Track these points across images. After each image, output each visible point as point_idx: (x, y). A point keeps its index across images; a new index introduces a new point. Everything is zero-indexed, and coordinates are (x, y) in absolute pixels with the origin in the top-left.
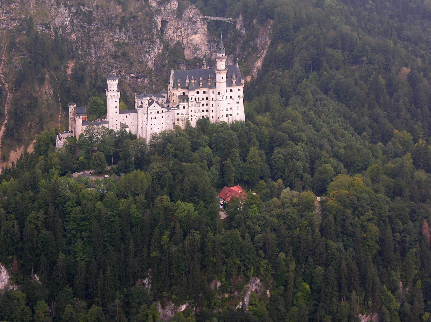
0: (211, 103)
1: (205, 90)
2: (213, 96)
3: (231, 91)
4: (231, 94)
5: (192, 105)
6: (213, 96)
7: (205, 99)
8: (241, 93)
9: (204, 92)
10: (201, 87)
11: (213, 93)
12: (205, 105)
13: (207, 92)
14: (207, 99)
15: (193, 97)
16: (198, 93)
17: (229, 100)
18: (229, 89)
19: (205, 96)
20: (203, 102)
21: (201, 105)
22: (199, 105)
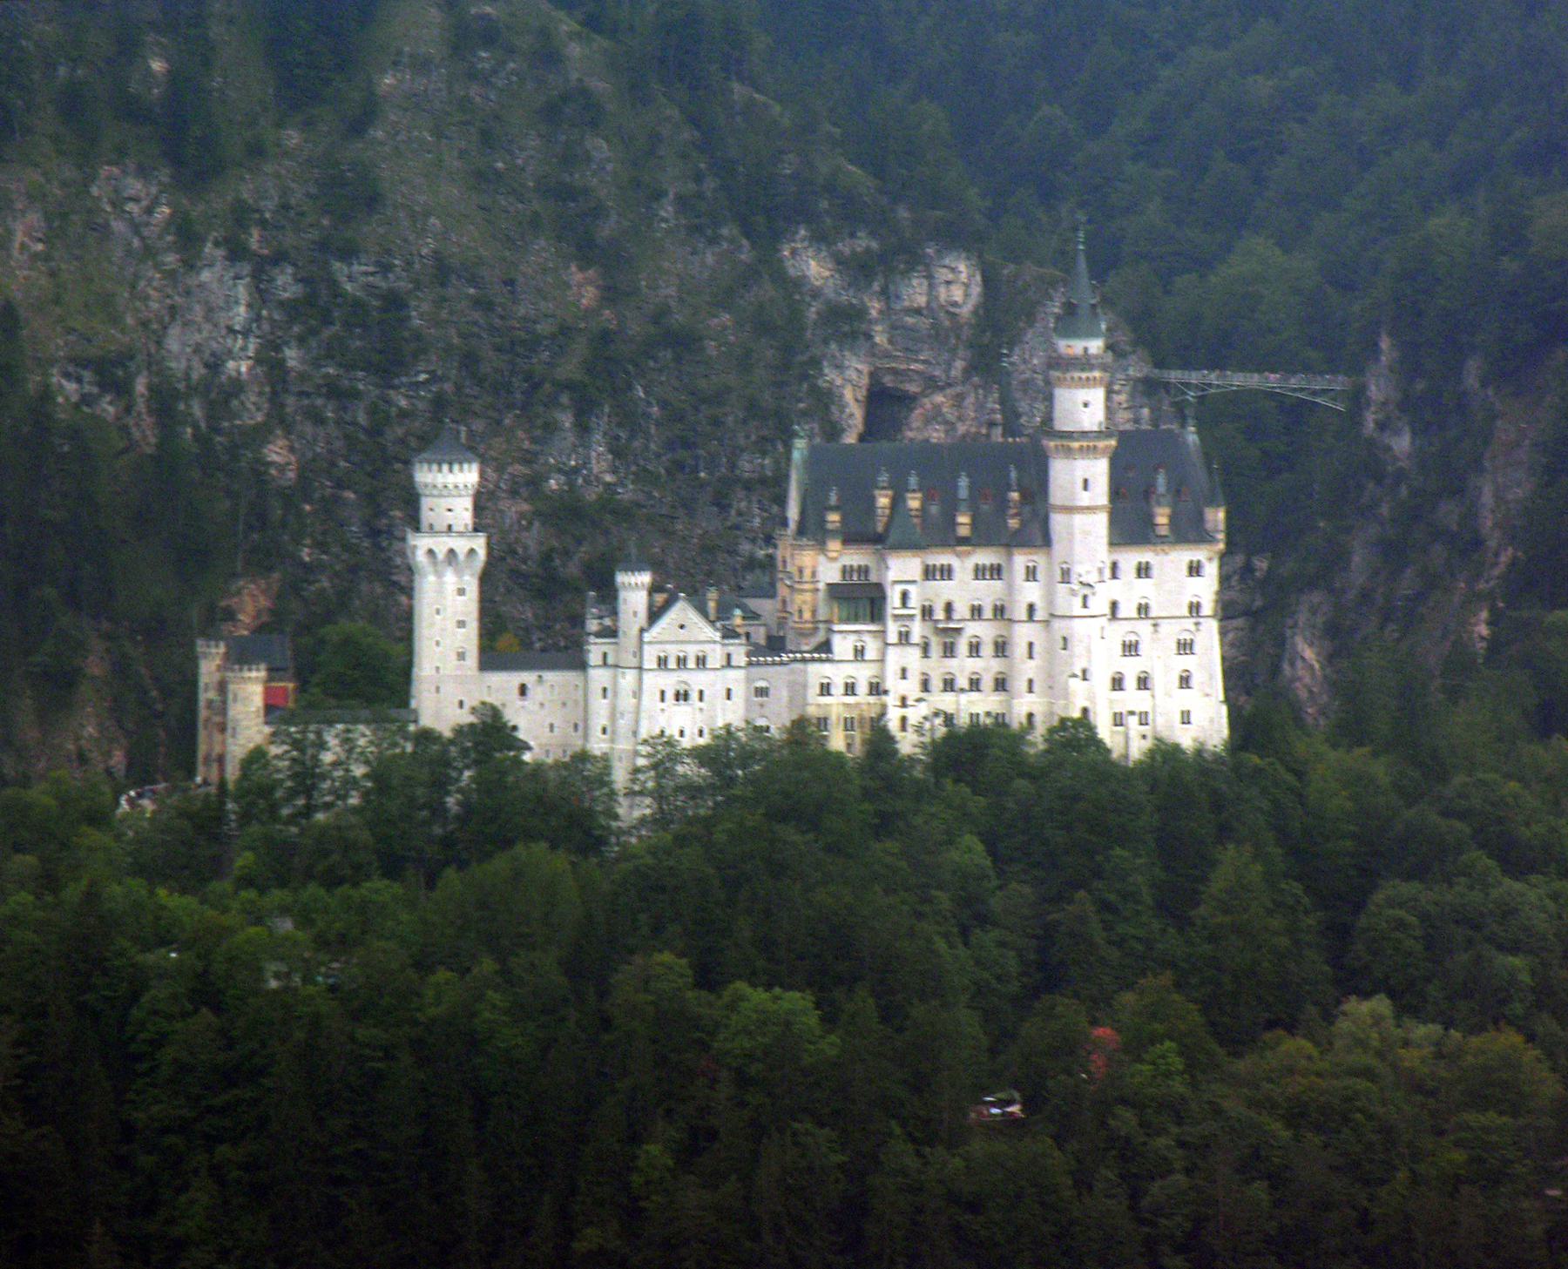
0: (1023, 634)
1: (985, 557)
2: (1031, 592)
3: (1143, 571)
4: (1144, 589)
5: (904, 638)
6: (1031, 592)
7: (988, 613)
8: (1206, 588)
9: (980, 572)
10: (964, 541)
11: (1031, 574)
12: (987, 649)
13: (996, 572)
14: (1000, 611)
15: (911, 588)
16: (946, 573)
17: (1127, 626)
18: (1130, 559)
19: (988, 592)
20: (973, 629)
21: (962, 647)
22: (949, 651)
